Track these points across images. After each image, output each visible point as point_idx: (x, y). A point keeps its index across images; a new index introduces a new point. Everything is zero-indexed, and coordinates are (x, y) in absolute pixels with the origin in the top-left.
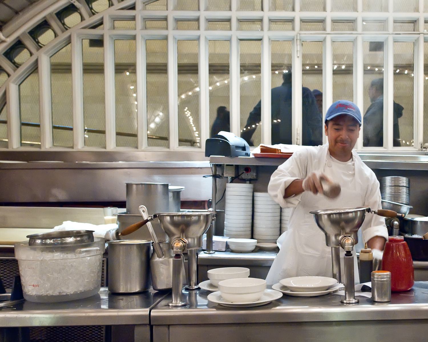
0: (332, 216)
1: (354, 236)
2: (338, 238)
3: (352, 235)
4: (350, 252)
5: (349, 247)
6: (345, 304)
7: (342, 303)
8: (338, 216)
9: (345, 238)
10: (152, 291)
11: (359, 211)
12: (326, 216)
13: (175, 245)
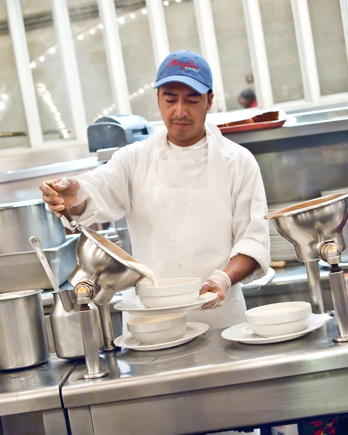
0: (299, 216)
1: (338, 241)
2: (314, 248)
3: (336, 239)
4: (337, 264)
5: (335, 259)
6: (340, 344)
7: (335, 343)
8: (308, 215)
9: (327, 246)
10: (54, 359)
11: (341, 200)
12: (291, 219)
13: (79, 292)
